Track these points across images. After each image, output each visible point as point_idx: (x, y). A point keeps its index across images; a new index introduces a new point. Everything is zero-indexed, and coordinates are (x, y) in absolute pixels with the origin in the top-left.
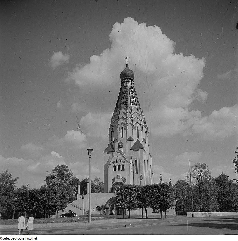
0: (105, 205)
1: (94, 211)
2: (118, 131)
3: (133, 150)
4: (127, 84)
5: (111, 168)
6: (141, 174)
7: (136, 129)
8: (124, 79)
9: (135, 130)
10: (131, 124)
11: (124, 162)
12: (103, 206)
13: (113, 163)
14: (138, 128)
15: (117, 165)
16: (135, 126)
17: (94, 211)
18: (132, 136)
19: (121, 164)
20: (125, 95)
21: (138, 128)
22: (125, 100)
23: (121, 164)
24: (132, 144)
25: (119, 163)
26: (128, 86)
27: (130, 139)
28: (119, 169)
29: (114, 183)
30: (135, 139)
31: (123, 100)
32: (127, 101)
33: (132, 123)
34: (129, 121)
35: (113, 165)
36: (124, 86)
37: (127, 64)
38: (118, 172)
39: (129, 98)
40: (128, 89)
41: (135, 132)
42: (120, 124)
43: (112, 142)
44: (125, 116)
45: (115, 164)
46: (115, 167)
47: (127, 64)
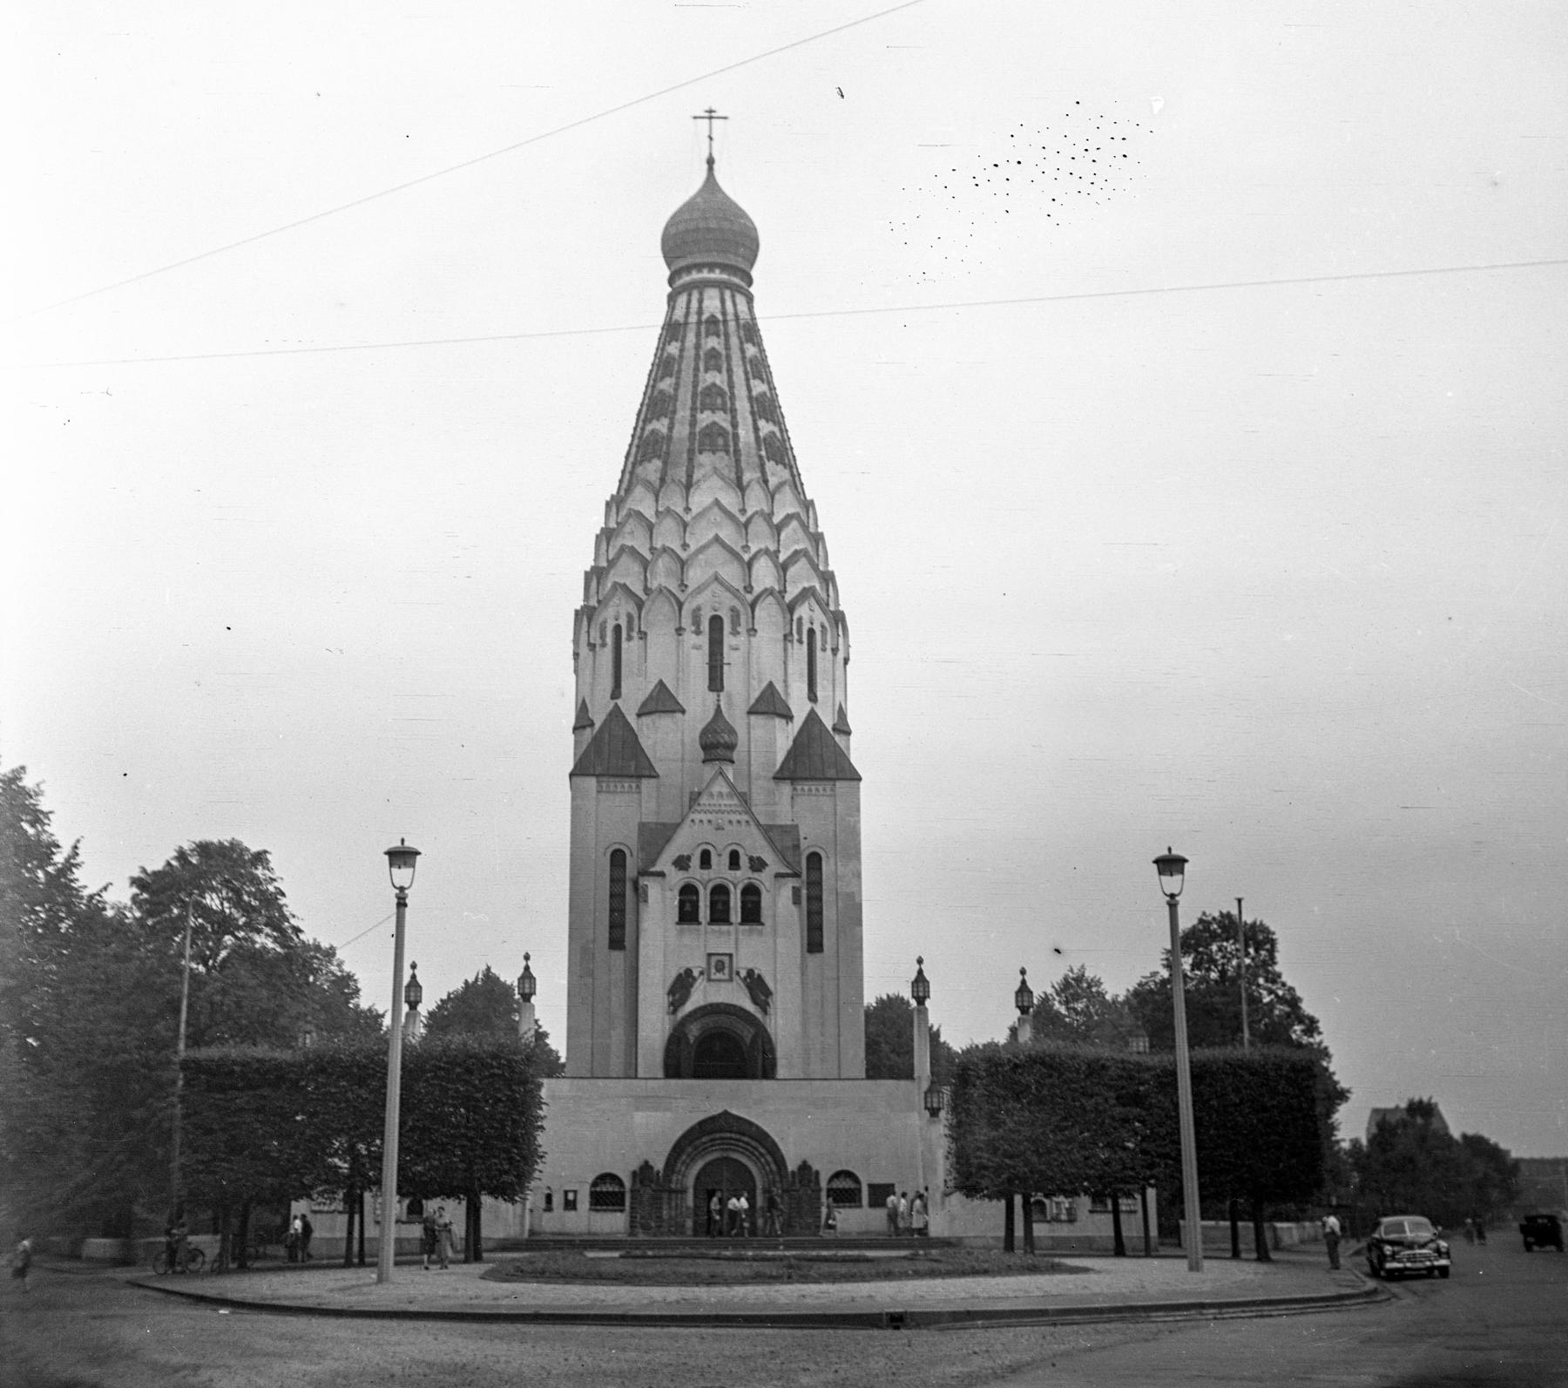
0: (659, 1165)
1: (570, 1205)
3: (793, 779)
4: (723, 301)
5: (660, 903)
6: (414, 966)
7: (805, 639)
8: (688, 269)
9: (800, 641)
11: (758, 865)
12: (644, 1172)
13: (682, 863)
14: (811, 632)
16: (800, 619)
17: (570, 1205)
18: (779, 687)
20: (719, 379)
21: (811, 632)
22: (722, 419)
24: (783, 737)
25: (720, 870)
27: (770, 704)
29: (689, 1007)
31: (705, 418)
32: (735, 425)
33: (783, 591)
34: (764, 575)
35: (677, 878)
36: (700, 312)
37: (710, 162)
39: (743, 406)
40: (734, 341)
41: (799, 652)
42: (699, 590)
43: (629, 707)
45: (696, 873)
46: (688, 892)
47: (710, 162)
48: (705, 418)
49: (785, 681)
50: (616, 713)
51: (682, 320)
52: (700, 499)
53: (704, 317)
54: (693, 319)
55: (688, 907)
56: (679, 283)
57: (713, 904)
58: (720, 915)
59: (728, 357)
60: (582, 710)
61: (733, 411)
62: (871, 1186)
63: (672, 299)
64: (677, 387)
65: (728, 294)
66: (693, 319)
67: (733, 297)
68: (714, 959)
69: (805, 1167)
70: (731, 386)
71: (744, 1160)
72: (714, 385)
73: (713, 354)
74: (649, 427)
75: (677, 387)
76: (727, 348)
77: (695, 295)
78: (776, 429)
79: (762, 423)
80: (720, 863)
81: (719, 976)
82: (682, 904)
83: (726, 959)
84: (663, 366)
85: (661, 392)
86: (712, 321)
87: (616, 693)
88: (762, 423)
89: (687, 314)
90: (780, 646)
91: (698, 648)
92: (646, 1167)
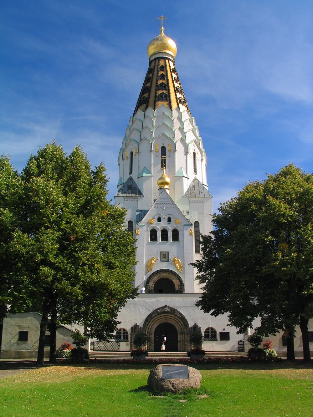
4: (165, 62)
14: (194, 154)
15: (159, 227)
21: (194, 154)
23: (170, 228)
25: (164, 224)
28: (165, 238)
36: (158, 65)
38: (161, 246)
43: (134, 176)
48: (160, 92)
49: (186, 167)
50: (131, 179)
51: (153, 68)
55: (153, 237)
56: (152, 59)
60: (120, 179)
62: (221, 333)
63: (150, 64)
64: (151, 85)
65: (167, 61)
66: (156, 67)
67: (169, 61)
68: (162, 254)
69: (195, 326)
70: (168, 83)
72: (163, 83)
74: (143, 97)
75: (151, 85)
77: (157, 61)
78: (182, 97)
79: (178, 94)
81: (164, 259)
83: (167, 254)
84: (148, 80)
85: (147, 86)
86: (162, 67)
87: (131, 172)
88: (178, 94)
89: (154, 67)
90: (185, 156)
91: (157, 156)
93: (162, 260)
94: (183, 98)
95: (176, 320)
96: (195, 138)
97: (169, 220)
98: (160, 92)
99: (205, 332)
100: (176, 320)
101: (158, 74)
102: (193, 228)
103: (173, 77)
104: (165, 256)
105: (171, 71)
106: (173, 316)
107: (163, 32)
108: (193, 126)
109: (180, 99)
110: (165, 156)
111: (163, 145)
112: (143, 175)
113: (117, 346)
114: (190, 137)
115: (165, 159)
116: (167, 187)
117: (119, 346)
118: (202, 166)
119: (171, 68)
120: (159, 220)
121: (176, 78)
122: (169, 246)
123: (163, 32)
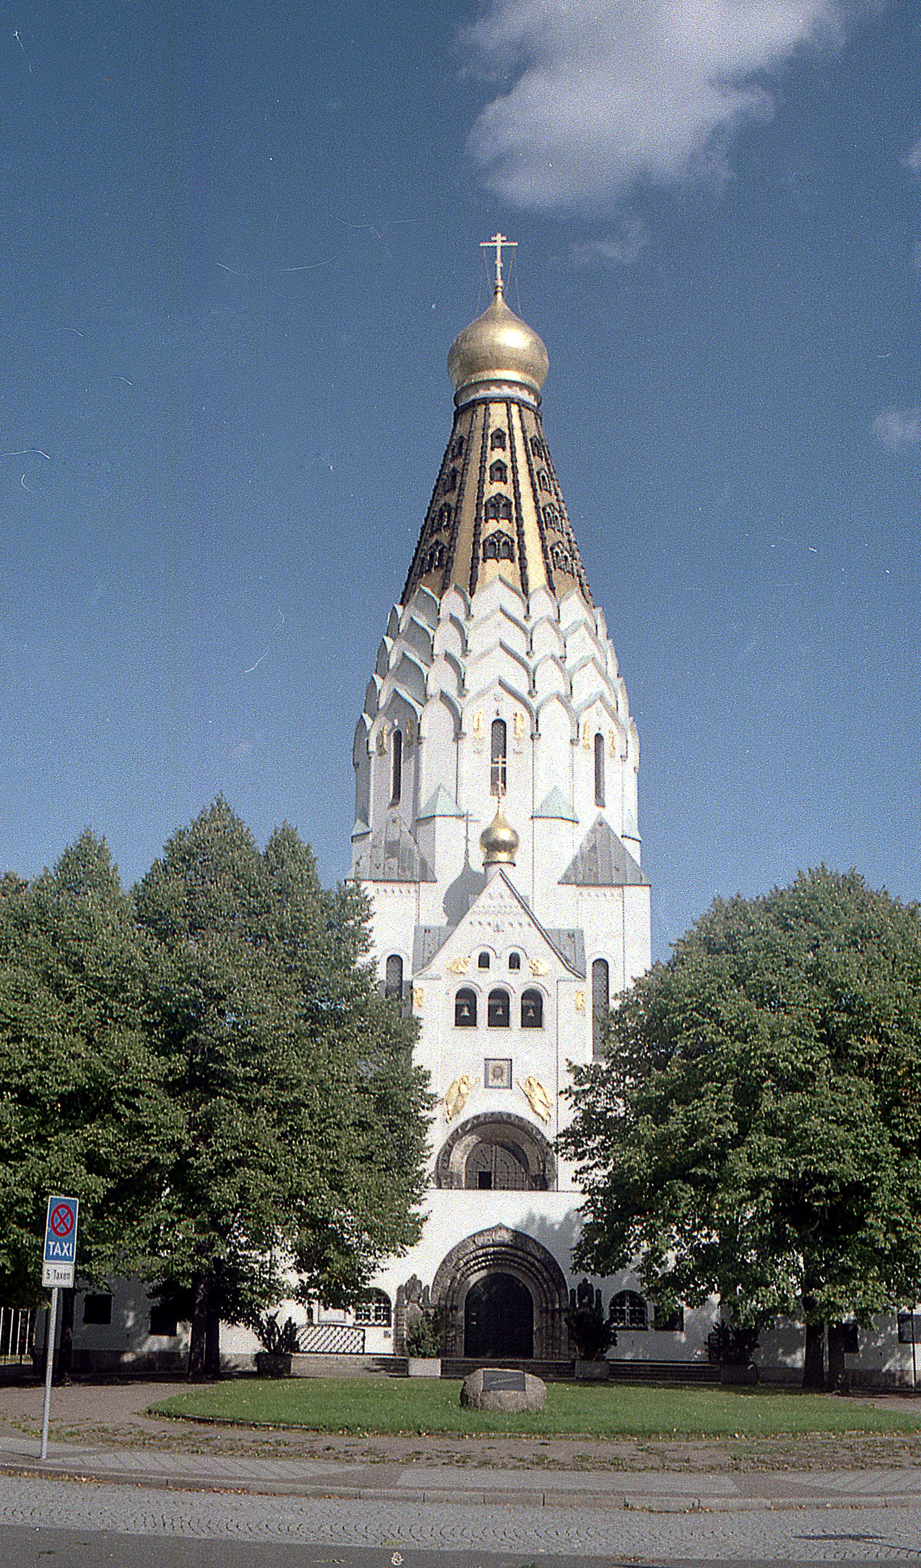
2: (466, 745)
10: (564, 700)
14: (599, 738)
19: (517, 984)
20: (506, 490)
21: (599, 738)
26: (518, 434)
30: (588, 814)
32: (521, 534)
34: (550, 680)
36: (485, 427)
38: (486, 1040)
44: (518, 644)
46: (466, 997)
48: (491, 527)
52: (482, 602)
53: (490, 432)
54: (478, 434)
57: (492, 1010)
58: (499, 1019)
59: (514, 468)
61: (520, 521)
65: (514, 409)
66: (478, 434)
67: (520, 411)
71: (519, 1276)
73: (499, 467)
76: (514, 460)
80: (499, 964)
81: (498, 1082)
82: (458, 1009)
86: (499, 436)
88: (548, 533)
92: (414, 1282)
93: (490, 1083)
94: (567, 545)
95: (528, 1266)
96: (603, 687)
97: (514, 962)
98: (491, 527)
99: (613, 1303)
100: (528, 1266)
101: (483, 459)
102: (587, 986)
103: (535, 473)
104: (499, 1072)
105: (527, 451)
106: (520, 1253)
107: (499, 295)
108: (597, 643)
109: (557, 549)
110: (504, 757)
111: (495, 717)
112: (438, 812)
113: (359, 1339)
114: (589, 684)
115: (504, 770)
116: (502, 856)
117: (363, 1339)
118: (622, 779)
119: (529, 436)
120: (484, 961)
121: (543, 473)
122: (512, 1041)
123: (499, 295)
